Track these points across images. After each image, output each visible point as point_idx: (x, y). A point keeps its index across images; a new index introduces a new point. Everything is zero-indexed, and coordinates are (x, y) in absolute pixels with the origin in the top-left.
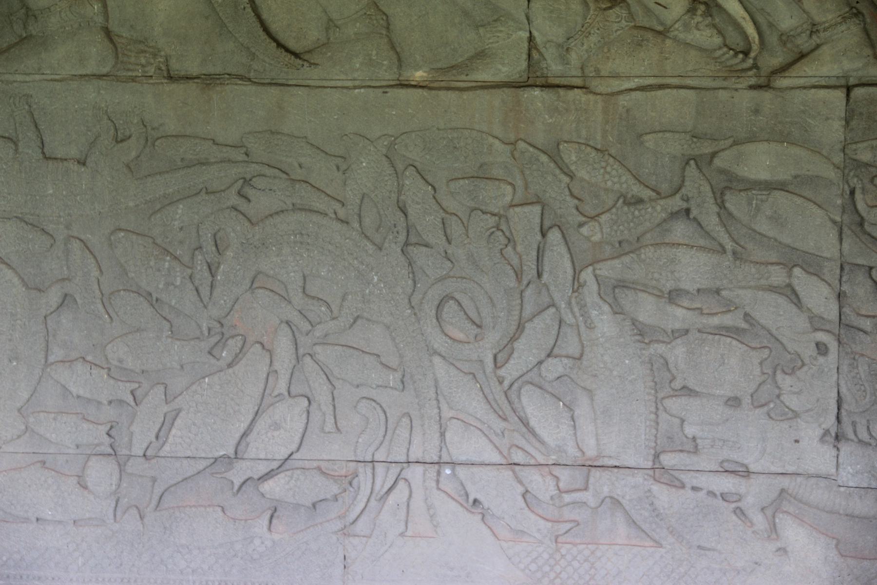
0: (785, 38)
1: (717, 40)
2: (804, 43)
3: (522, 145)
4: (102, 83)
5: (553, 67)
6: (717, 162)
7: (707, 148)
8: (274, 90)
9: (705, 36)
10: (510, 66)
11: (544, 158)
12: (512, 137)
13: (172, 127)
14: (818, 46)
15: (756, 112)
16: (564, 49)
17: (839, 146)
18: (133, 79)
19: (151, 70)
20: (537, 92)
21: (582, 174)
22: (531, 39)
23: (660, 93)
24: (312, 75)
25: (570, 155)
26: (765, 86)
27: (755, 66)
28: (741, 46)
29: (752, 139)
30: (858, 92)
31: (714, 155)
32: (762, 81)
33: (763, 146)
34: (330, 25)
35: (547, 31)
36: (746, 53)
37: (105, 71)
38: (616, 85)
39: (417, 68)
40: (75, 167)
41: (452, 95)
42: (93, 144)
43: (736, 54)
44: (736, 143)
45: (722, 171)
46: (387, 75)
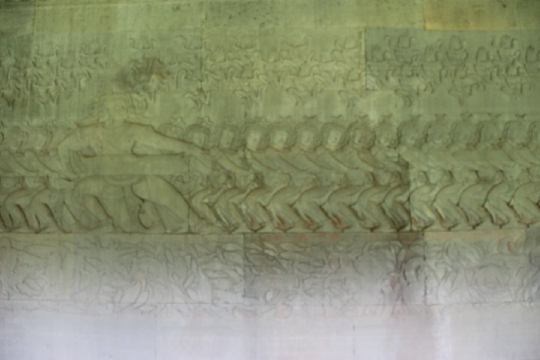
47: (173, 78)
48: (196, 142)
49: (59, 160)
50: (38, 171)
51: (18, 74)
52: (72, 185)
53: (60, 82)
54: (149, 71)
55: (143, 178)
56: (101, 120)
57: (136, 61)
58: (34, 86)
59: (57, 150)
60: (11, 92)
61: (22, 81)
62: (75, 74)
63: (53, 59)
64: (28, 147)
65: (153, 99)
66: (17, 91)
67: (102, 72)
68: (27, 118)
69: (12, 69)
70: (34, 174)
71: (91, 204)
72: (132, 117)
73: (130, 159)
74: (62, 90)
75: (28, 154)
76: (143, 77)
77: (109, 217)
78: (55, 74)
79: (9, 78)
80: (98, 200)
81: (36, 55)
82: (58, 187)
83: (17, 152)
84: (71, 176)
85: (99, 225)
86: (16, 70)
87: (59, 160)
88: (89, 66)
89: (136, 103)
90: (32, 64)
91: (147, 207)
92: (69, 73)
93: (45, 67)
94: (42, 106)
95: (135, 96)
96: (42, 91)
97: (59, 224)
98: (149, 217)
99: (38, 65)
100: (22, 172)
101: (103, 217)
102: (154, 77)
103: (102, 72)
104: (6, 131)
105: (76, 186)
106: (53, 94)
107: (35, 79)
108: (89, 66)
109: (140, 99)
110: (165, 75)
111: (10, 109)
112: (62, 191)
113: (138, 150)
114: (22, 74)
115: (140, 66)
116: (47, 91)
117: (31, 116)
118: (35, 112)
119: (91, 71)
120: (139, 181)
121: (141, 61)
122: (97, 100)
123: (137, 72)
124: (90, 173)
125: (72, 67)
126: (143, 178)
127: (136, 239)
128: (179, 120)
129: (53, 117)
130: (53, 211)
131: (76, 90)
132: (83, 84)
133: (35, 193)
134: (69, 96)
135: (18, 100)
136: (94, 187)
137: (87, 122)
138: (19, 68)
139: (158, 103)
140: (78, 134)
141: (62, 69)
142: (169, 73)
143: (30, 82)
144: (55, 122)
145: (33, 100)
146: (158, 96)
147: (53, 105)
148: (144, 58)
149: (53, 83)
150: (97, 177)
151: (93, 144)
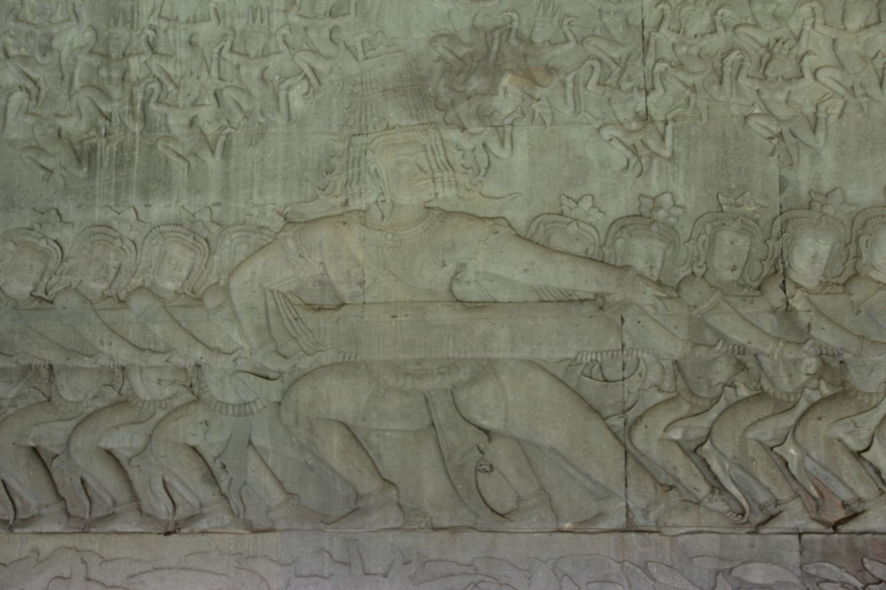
0: (762, 507)
1: (727, 508)
2: (773, 510)
3: (626, 564)
4: (396, 532)
5: (640, 521)
6: (734, 573)
7: (727, 566)
8: (490, 535)
9: (719, 505)
10: (618, 521)
11: (639, 571)
12: (621, 559)
13: (434, 555)
14: (780, 512)
15: (752, 546)
16: (646, 512)
17: (798, 566)
18: (414, 530)
19: (423, 525)
20: (633, 535)
21: (661, 579)
22: (627, 506)
23: (699, 535)
24: (511, 526)
25: (653, 569)
26: (755, 532)
27: (748, 522)
28: (739, 510)
29: (751, 561)
30: (805, 537)
31: (731, 569)
32: (753, 529)
33: (758, 565)
34: (519, 499)
35: (636, 502)
36: (743, 514)
37: (398, 525)
38: (676, 531)
39: (567, 521)
40: (381, 579)
41: (587, 536)
42: (391, 566)
43: (738, 515)
44: (743, 563)
45: (736, 578)
46: (551, 526)
47: (564, 84)
48: (640, 265)
49: (235, 317)
50: (169, 350)
51: (103, 73)
52: (273, 391)
53: (229, 95)
54: (493, 69)
55: (486, 369)
56: (357, 204)
57: (452, 37)
58: (152, 106)
59: (226, 289)
60: (83, 127)
61: (116, 93)
62: (272, 74)
63: (207, 31)
64: (137, 281)
65: (507, 145)
66: (101, 121)
67: (352, 68)
68: (134, 199)
69: (83, 58)
70: (157, 360)
71: (333, 445)
72: (447, 195)
73: (446, 315)
74: (238, 117)
75: (139, 303)
76: (476, 83)
77: (388, 483)
78: (214, 74)
79: (77, 84)
80: (350, 432)
81: (154, 21)
82: (231, 399)
83: (105, 297)
84: (273, 364)
85: (357, 507)
86: (95, 61)
87: (235, 317)
88: (316, 52)
89: (456, 157)
90: (144, 47)
91: (500, 453)
92: (256, 72)
93: (183, 53)
94: (178, 164)
95: (454, 135)
96: (176, 121)
97: (235, 501)
98: (506, 483)
99: (161, 49)
100: (124, 354)
101: (369, 484)
102: (506, 81)
103: (352, 68)
104: (67, 235)
105: (285, 393)
106: (210, 130)
107: (155, 86)
108: (316, 52)
109: (468, 144)
110: (539, 76)
111: (83, 172)
112: (243, 409)
113: (469, 291)
114: (116, 74)
115: (462, 51)
116: (192, 123)
117: (145, 192)
118: (156, 182)
119: (322, 66)
120: (474, 380)
121: (466, 37)
122: (340, 147)
123: (458, 70)
124: (329, 356)
125: (265, 53)
126: (486, 369)
127: (470, 548)
128: (586, 204)
129: (213, 197)
130: (216, 467)
131: (280, 119)
132: (298, 104)
133: (160, 414)
134: (259, 136)
135: (107, 149)
136: (341, 397)
137: (314, 209)
138: (106, 56)
139: (521, 158)
140: (291, 243)
141: (235, 59)
142: (550, 70)
143: (139, 97)
144: (216, 210)
145: (152, 147)
146: (522, 137)
147: (213, 162)
148: (474, 28)
149: (210, 100)
150: (348, 366)
151: (333, 272)
